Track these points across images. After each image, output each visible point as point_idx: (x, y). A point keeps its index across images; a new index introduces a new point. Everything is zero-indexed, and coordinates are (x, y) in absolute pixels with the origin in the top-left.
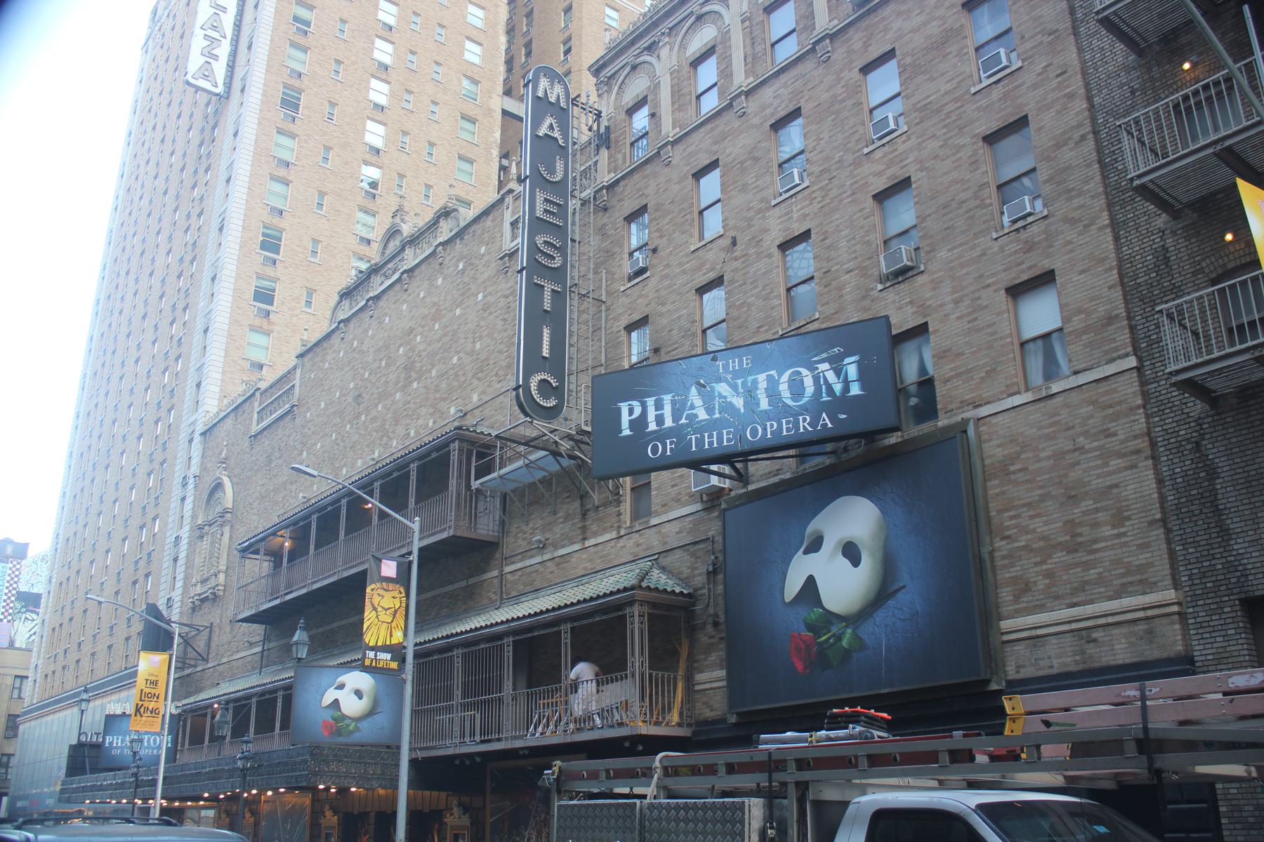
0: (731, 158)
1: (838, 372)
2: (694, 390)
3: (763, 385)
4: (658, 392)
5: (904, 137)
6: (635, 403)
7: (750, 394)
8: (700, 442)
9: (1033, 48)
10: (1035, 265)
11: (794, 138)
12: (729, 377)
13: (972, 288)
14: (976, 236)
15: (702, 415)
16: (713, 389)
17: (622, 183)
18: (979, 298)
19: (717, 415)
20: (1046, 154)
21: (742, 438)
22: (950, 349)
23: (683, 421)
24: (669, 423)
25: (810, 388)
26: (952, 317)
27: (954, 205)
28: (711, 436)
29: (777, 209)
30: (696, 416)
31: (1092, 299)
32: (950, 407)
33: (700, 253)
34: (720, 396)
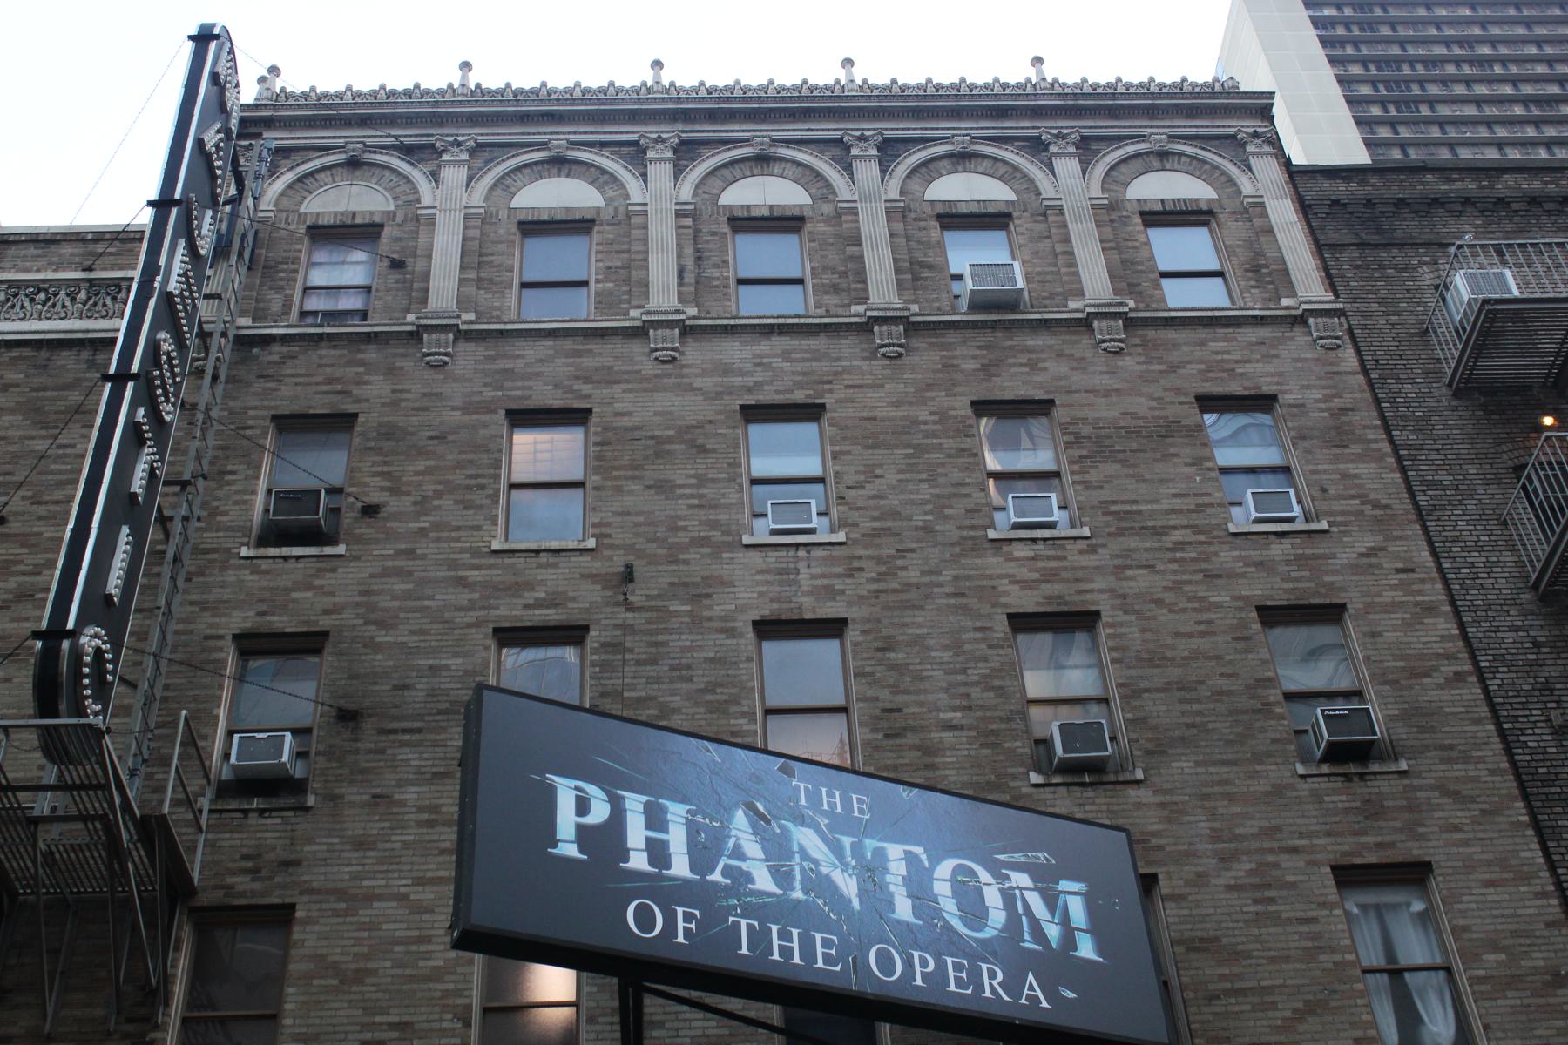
0: (625, 422)
1: (1051, 901)
2: (740, 819)
3: (897, 868)
4: (657, 788)
5: (1082, 545)
6: (593, 790)
7: (871, 872)
8: (760, 939)
9: (1343, 513)
10: (1392, 845)
11: (785, 452)
12: (824, 822)
13: (1256, 845)
14: (1258, 758)
15: (763, 881)
17: (276, 348)
18: (1276, 865)
19: (798, 894)
20: (1390, 677)
21: (860, 965)
22: (1216, 939)
23: (716, 876)
24: (680, 867)
25: (998, 917)
26: (1213, 881)
27: (1204, 692)
28: (785, 935)
29: (752, 553)
30: (749, 878)
31: (1515, 934)
33: (519, 561)
34: (805, 855)
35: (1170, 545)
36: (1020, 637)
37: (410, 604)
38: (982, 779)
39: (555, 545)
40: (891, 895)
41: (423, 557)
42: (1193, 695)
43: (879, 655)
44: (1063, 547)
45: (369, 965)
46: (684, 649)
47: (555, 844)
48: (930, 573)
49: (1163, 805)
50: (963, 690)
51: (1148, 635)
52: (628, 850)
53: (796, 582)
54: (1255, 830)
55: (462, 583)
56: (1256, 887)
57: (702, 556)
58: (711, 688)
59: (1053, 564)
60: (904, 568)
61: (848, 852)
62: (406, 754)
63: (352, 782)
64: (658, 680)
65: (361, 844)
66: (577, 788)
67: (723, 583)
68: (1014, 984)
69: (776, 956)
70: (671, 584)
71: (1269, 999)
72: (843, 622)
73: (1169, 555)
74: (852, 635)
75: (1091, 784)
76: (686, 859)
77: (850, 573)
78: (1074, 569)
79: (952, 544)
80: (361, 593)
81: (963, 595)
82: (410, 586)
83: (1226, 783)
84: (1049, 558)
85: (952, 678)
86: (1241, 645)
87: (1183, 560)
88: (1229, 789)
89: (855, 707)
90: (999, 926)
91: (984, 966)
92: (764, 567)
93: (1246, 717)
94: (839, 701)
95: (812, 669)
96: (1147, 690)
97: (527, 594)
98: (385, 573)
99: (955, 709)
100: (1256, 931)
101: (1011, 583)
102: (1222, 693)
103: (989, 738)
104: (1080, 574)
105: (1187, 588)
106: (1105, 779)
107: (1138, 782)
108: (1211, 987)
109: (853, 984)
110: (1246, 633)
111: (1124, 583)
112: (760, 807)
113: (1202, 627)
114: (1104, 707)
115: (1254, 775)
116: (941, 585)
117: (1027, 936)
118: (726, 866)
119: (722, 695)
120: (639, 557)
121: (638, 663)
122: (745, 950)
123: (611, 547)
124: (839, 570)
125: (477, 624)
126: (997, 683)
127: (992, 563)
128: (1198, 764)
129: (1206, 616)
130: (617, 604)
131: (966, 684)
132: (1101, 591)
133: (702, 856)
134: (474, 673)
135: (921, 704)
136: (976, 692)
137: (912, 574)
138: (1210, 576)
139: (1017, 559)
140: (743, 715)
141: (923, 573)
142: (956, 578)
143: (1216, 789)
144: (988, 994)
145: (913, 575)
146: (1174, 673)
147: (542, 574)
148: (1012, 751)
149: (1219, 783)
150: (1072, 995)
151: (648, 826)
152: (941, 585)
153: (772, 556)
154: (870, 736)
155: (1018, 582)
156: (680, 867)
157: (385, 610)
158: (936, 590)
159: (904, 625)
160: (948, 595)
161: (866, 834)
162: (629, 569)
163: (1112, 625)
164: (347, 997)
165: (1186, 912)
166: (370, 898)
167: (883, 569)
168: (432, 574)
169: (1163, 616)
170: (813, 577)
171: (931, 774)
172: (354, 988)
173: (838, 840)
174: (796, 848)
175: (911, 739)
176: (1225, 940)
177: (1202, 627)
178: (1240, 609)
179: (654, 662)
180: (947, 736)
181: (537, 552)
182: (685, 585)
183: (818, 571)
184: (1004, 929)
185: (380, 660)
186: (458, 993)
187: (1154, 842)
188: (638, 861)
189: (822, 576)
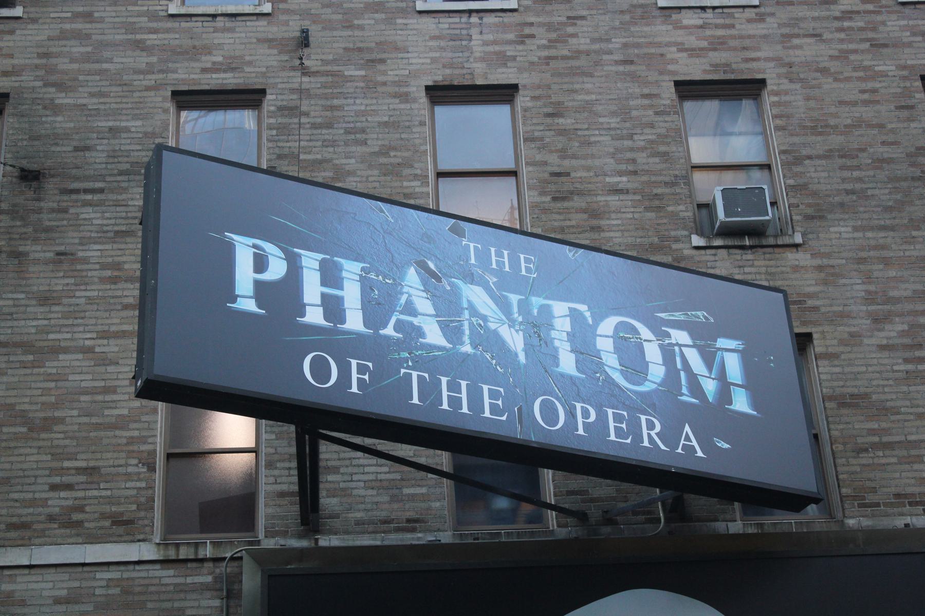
1: (709, 358)
2: (412, 277)
3: (562, 325)
4: (333, 247)
6: (270, 248)
7: (537, 329)
8: (430, 390)
13: (909, 307)
15: (434, 336)
16: (455, 292)
19: (467, 348)
21: (524, 415)
22: (866, 396)
23: (389, 331)
24: (354, 322)
25: (657, 372)
26: (866, 341)
27: (864, 158)
28: (454, 387)
30: (420, 332)
32: (871, 498)
34: (474, 312)
35: (838, 14)
36: (688, 105)
37: (87, 66)
38: (646, 241)
39: (231, 9)
40: (556, 350)
41: (101, 20)
42: (855, 162)
43: (549, 120)
44: (732, 16)
45: (57, 414)
46: (358, 114)
47: (234, 298)
48: (600, 40)
49: (820, 268)
50: (629, 155)
51: (812, 104)
52: (304, 305)
53: (468, 48)
54: (908, 293)
55: (139, 46)
56: (911, 347)
57: (377, 21)
58: (384, 152)
59: (720, 32)
60: (574, 35)
61: (515, 309)
62: (88, 213)
63: (36, 240)
64: (333, 143)
65: (46, 299)
66: (255, 246)
67: (397, 49)
68: (671, 435)
69: (445, 406)
70: (345, 49)
71: (913, 452)
72: (514, 88)
73: (837, 24)
74: (522, 100)
75: (751, 247)
76: (360, 314)
77: (522, 39)
78: (741, 37)
79: (622, 12)
80: (40, 56)
81: (632, 62)
82: (89, 49)
83: (883, 247)
84: (717, 26)
85: (618, 143)
86: (905, 113)
87: (851, 29)
88: (885, 253)
89: (524, 171)
90: (658, 380)
91: (643, 418)
92: (437, 33)
93: (904, 184)
94: (510, 165)
95: (481, 134)
96: (810, 157)
97: (204, 58)
98: (64, 36)
99: (620, 174)
100: (905, 388)
101: (680, 50)
102: (883, 161)
103: (653, 202)
104: (747, 43)
105: (852, 57)
106: (764, 242)
107: (796, 246)
108: (860, 440)
109: (519, 433)
110: (910, 102)
111: (791, 52)
112: (432, 265)
113: (866, 96)
114: (766, 172)
115: (911, 240)
116: (610, 53)
117: (684, 390)
118: (398, 321)
119: (395, 157)
120: (314, 22)
121: (314, 126)
122: (415, 400)
123: (287, 12)
124: (511, 36)
125: (156, 88)
126: (662, 148)
127: (661, 30)
128: (856, 229)
129: (870, 85)
130: (293, 69)
131: (632, 149)
132: (767, 59)
133: (375, 311)
134: (153, 135)
135: (588, 169)
136: (641, 158)
137: (582, 41)
138: (877, 46)
139: (686, 27)
140: (416, 177)
141: (594, 41)
142: (625, 45)
143: (872, 253)
144: (646, 443)
145: (582, 43)
146: (836, 140)
147: (219, 38)
148: (674, 215)
149: (876, 248)
150: (726, 446)
151: (324, 283)
152: (610, 53)
153: (446, 21)
154: (538, 199)
155: (686, 50)
156: (354, 322)
157: (64, 72)
158: (605, 57)
159: (575, 91)
160: (617, 63)
161: (533, 292)
162: (305, 33)
163: (776, 94)
164: (35, 444)
165: (837, 370)
166: (56, 350)
167: (554, 36)
168: (111, 37)
169: (828, 84)
170: (486, 43)
171: (596, 236)
172: (43, 436)
173: (506, 298)
174: (465, 305)
175: (578, 202)
176: (874, 397)
177: (866, 96)
178: (904, 78)
179: (329, 126)
180: (614, 200)
181: (214, 16)
182: (360, 50)
183: (490, 37)
184: (663, 383)
185: (61, 123)
186: (143, 440)
187: (810, 303)
188: (314, 316)
189: (495, 42)
